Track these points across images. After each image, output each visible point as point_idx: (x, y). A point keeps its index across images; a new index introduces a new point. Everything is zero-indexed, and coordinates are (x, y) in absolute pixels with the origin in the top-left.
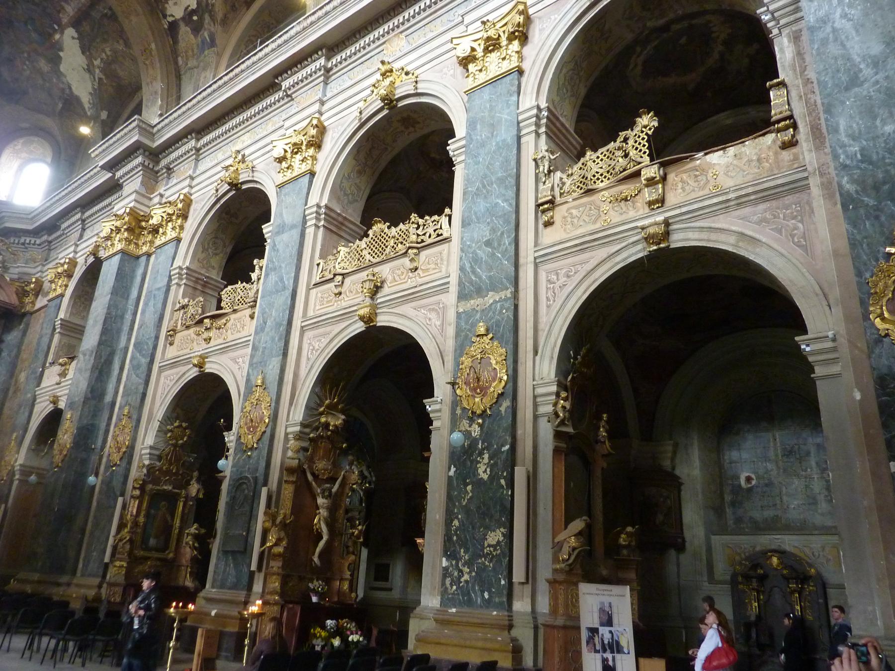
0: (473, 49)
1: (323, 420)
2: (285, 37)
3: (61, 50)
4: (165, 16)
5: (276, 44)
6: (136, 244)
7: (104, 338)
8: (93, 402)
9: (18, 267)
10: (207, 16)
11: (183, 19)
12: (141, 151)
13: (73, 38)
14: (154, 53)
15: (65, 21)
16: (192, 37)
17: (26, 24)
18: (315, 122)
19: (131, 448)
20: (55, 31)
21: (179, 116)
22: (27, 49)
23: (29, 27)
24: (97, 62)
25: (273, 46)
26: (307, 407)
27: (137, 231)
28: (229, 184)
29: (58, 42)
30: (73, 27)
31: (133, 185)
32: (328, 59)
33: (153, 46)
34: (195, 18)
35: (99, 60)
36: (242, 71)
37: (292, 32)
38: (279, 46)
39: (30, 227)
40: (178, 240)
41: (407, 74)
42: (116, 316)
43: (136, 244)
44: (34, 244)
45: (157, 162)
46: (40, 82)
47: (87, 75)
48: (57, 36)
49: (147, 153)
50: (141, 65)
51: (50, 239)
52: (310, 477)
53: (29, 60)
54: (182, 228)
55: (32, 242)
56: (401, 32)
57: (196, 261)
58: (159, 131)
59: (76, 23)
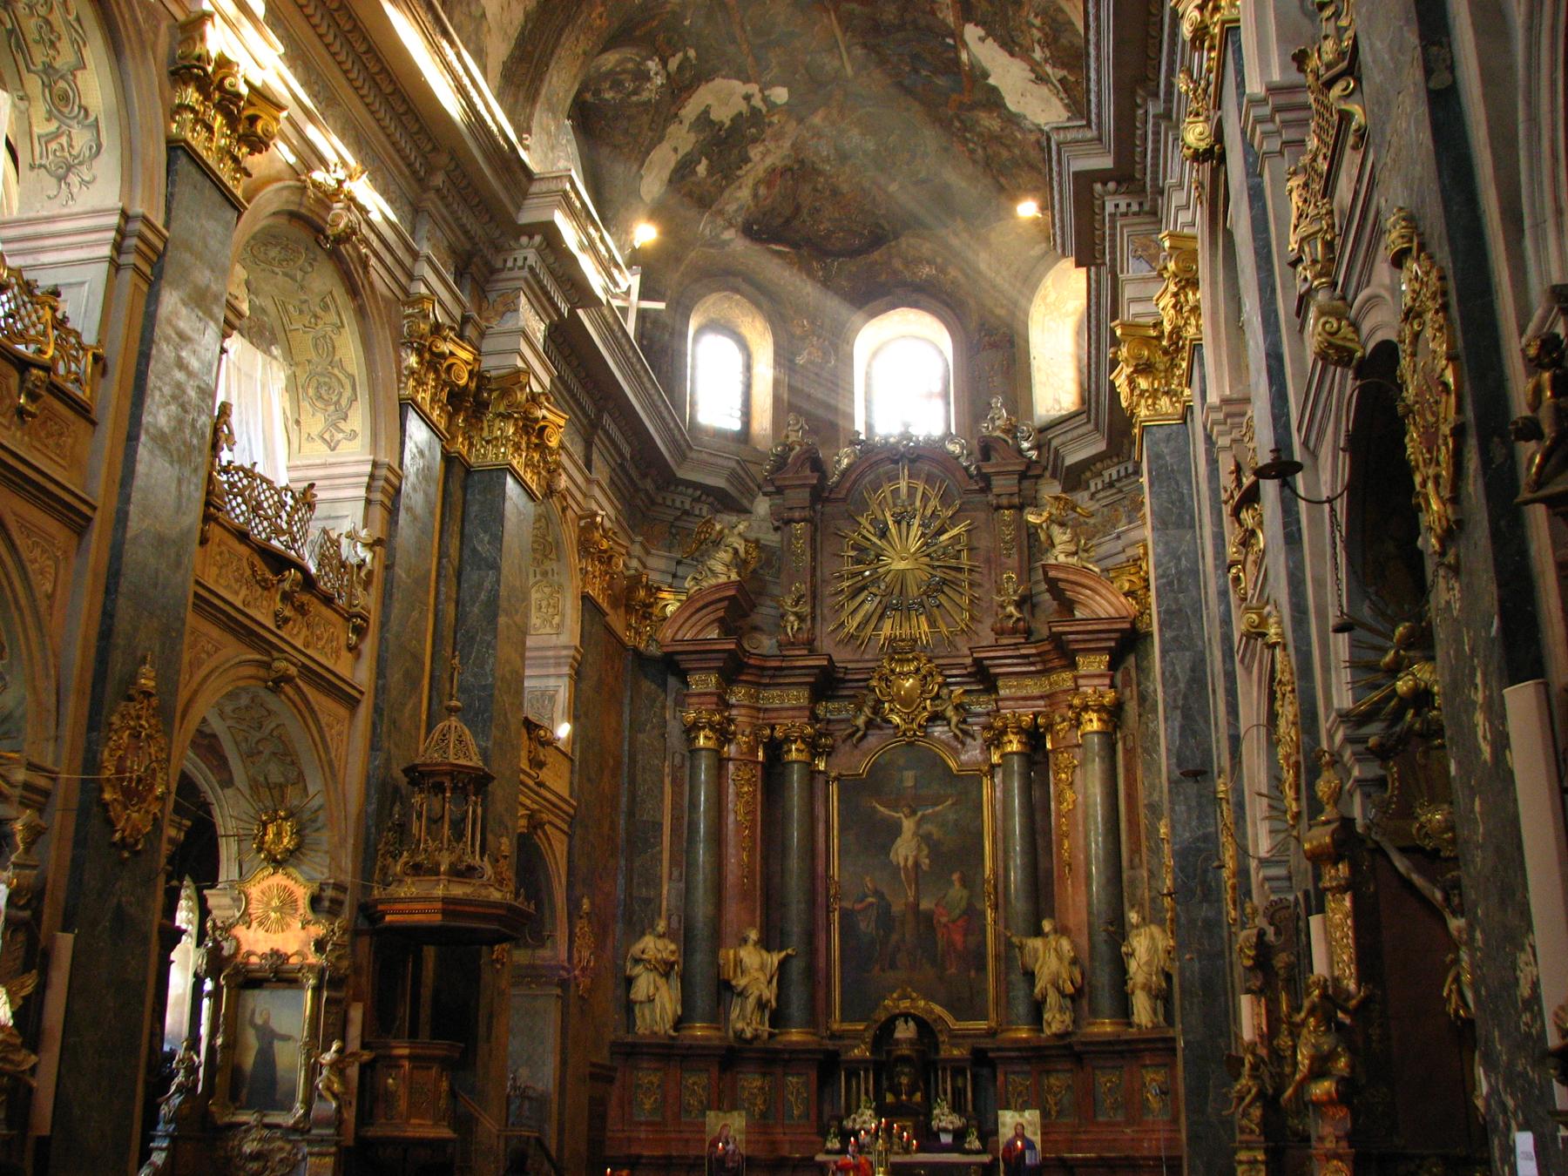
1: (1402, 686)
3: (986, 75)
7: (1168, 635)
8: (1191, 788)
9: (1118, 537)
12: (1098, 187)
13: (982, 40)
15: (951, 20)
17: (917, 72)
19: (1242, 873)
20: (955, 48)
22: (951, 113)
23: (924, 73)
24: (1038, 55)
26: (1354, 664)
27: (1162, 367)
29: (972, 66)
30: (969, 21)
35: (1037, 47)
39: (1101, 446)
40: (1196, 347)
42: (1180, 573)
44: (1127, 476)
45: (1144, 190)
46: (1005, 154)
47: (1044, 90)
48: (964, 56)
49: (1111, 186)
52: (1401, 863)
53: (966, 130)
54: (1195, 309)
55: (1122, 473)
59: (967, 12)
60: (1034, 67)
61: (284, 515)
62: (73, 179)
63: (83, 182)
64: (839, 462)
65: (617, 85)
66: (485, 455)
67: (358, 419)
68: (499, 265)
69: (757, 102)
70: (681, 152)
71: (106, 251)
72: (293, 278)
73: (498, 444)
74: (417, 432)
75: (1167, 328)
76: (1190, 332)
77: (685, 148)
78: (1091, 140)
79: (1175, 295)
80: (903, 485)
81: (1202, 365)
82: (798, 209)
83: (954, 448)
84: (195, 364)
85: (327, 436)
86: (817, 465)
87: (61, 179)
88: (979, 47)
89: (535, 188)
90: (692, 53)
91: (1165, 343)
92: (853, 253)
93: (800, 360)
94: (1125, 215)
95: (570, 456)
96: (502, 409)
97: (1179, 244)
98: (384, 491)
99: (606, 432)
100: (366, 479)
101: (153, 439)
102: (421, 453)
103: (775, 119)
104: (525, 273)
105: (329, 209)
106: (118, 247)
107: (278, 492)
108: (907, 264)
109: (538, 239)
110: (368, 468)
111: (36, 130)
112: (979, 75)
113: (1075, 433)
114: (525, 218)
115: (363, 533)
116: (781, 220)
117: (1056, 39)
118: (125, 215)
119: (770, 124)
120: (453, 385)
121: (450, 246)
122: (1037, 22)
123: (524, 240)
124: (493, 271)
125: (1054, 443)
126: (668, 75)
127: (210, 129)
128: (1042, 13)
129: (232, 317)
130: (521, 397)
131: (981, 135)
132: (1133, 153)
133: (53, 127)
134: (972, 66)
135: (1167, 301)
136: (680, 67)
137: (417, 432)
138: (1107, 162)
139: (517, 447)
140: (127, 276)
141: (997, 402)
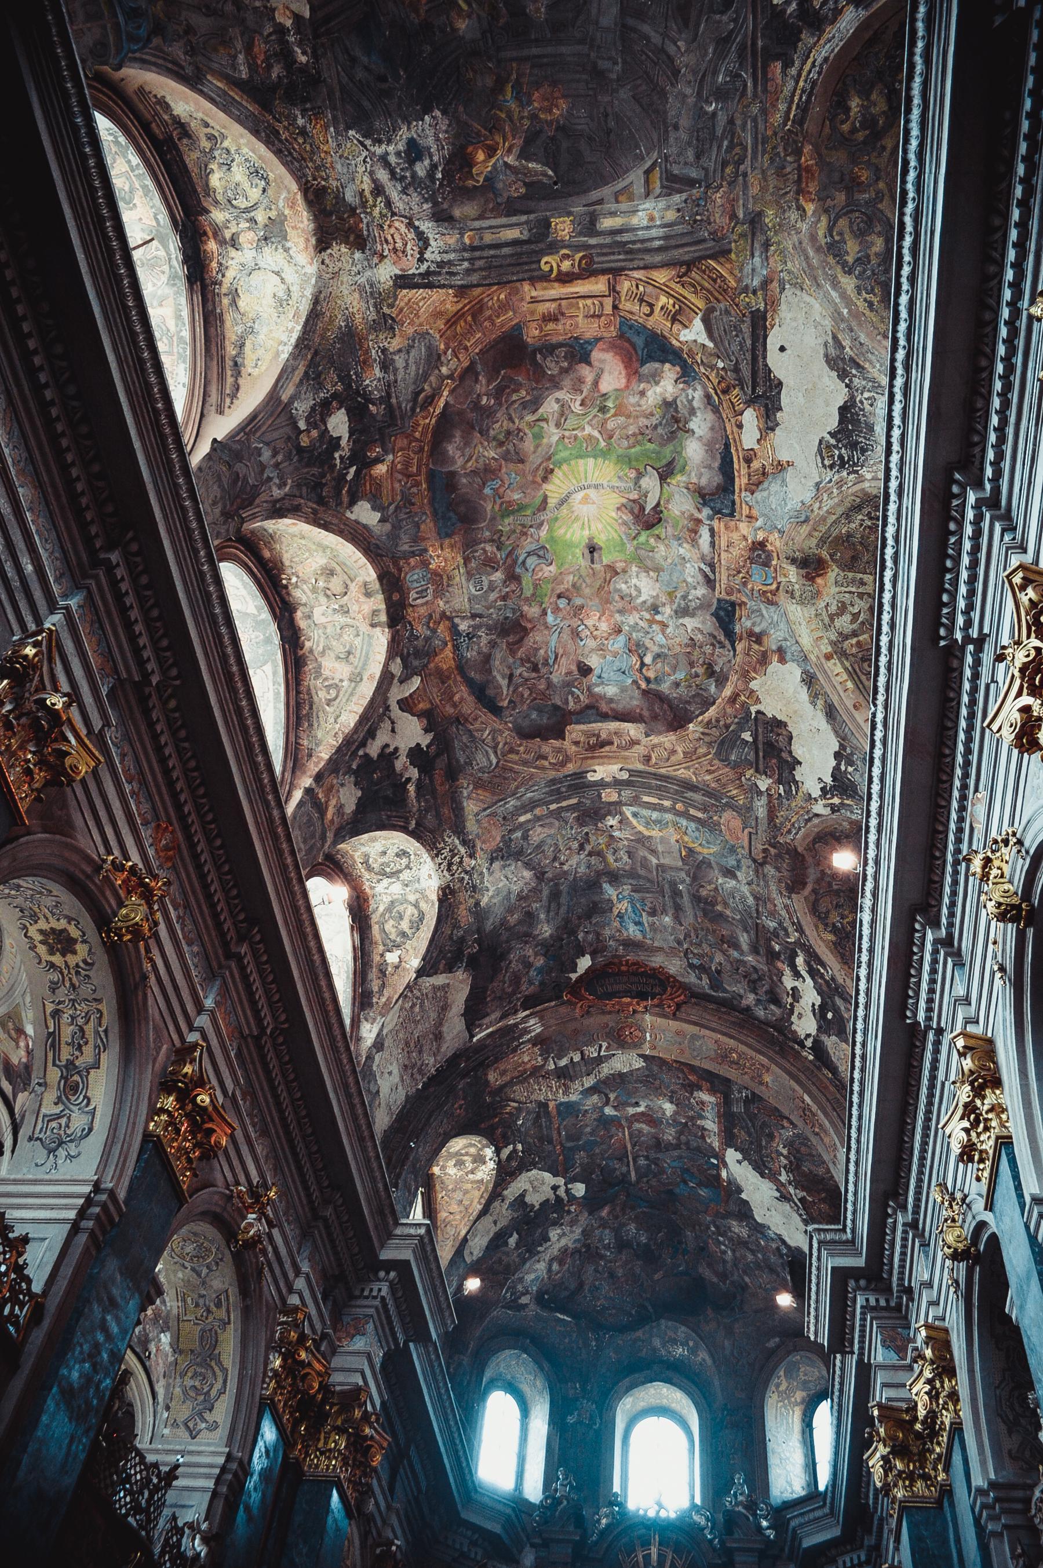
0: (1026, 710)
2: (865, 945)
3: (740, 1190)
4: (803, 1046)
5: (864, 966)
6: (926, 1477)
10: (838, 1001)
11: (820, 1029)
12: (852, 1283)
14: (814, 1108)
15: (716, 1145)
16: (844, 1045)
17: (685, 1182)
18: (960, 1043)
20: (717, 1167)
21: (856, 1185)
24: (783, 1178)
25: (863, 972)
27: (915, 1450)
28: (956, 1256)
29: (729, 1182)
31: (880, 1355)
32: (936, 924)
33: (806, 1098)
34: (830, 1015)
36: (864, 1045)
37: (866, 931)
38: (870, 964)
39: (836, 1532)
40: (957, 1428)
41: (1006, 842)
43: (926, 1477)
45: (889, 1289)
46: (750, 1257)
47: (787, 1207)
48: (724, 1174)
49: (862, 1283)
50: (814, 1140)
51: (873, 1542)
54: (954, 1396)
56: (976, 790)
57: (1007, 1459)
58: (853, 1231)
59: (729, 1140)
60: (780, 1186)
61: (146, 1494)
62: (62, 1153)
63: (70, 1157)
64: (599, 1521)
65: (460, 1164)
66: (317, 1466)
67: (222, 1412)
68: (357, 1293)
69: (561, 1192)
70: (499, 1226)
71: (72, 1214)
72: (199, 1275)
73: (328, 1458)
74: (269, 1433)
75: (921, 1412)
76: (947, 1418)
77: (503, 1223)
78: (847, 1241)
79: (929, 1382)
80: (654, 1557)
81: (963, 1448)
82: (581, 1285)
83: (699, 1519)
84: (115, 1329)
85: (191, 1425)
86: (579, 1521)
87: (51, 1151)
88: (736, 1167)
89: (398, 1231)
90: (520, 1147)
91: (918, 1426)
92: (623, 1329)
93: (571, 1420)
94: (873, 1309)
95: (379, 1480)
96: (339, 1423)
97: (933, 1334)
98: (230, 1486)
99: (411, 1466)
100: (217, 1471)
101: (62, 1392)
102: (267, 1452)
103: (573, 1208)
104: (377, 1302)
105: (245, 1218)
106: (82, 1213)
107: (147, 1468)
108: (664, 1346)
109: (392, 1274)
110: (221, 1460)
111: (43, 1111)
112: (733, 1189)
113: (811, 1516)
114: (385, 1255)
115: (204, 1526)
116: (566, 1293)
117: (798, 1167)
118: (97, 1187)
119: (569, 1212)
120: (305, 1393)
121: (323, 1269)
122: (785, 1152)
123: (382, 1274)
124: (352, 1297)
125: (793, 1524)
126: (499, 1163)
127: (177, 1131)
128: (789, 1144)
129: (152, 1292)
130: (358, 1414)
131: (731, 1239)
132: (882, 1255)
133: (61, 1107)
134: (729, 1182)
135: (920, 1388)
136: (510, 1157)
137: (269, 1433)
138: (860, 1262)
139: (345, 1463)
140: (82, 1238)
141: (739, 1478)
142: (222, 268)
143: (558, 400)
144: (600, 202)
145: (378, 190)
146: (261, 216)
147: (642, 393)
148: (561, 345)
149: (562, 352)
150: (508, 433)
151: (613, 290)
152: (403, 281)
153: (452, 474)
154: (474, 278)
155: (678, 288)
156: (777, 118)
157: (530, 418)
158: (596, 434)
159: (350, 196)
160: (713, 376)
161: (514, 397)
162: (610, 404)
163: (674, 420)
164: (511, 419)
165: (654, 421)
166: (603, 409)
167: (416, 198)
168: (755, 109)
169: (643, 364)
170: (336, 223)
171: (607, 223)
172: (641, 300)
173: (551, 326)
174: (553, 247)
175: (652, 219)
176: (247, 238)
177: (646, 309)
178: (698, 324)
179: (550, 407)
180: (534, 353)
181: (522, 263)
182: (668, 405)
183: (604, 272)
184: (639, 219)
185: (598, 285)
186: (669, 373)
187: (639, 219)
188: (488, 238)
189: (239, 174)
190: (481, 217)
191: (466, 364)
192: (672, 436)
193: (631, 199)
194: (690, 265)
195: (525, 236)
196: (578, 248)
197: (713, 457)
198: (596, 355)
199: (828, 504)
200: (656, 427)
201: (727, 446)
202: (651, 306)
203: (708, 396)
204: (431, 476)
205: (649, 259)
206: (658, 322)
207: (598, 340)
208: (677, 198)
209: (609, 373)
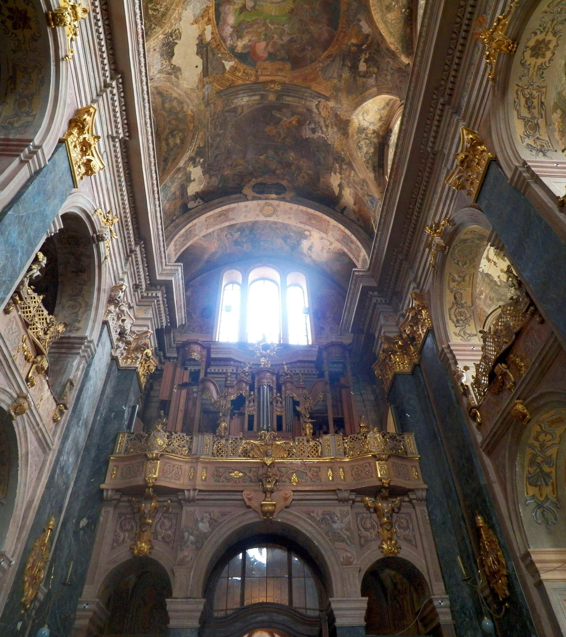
142: (381, 127)
143: (283, 40)
144: (258, 104)
145: (327, 126)
146: (364, 136)
147: (250, 41)
148: (278, 60)
149: (278, 58)
150: (303, 33)
151: (257, 77)
152: (327, 99)
153: (328, 25)
154: (304, 90)
155: (234, 79)
156: (201, 134)
157: (294, 36)
158: (270, 25)
159: (336, 129)
160: (222, 50)
161: (299, 46)
162: (263, 37)
163: (238, 31)
164: (301, 38)
165: (246, 30)
166: (266, 35)
167: (316, 119)
168: (208, 134)
169: (249, 52)
170: (343, 125)
171: (257, 98)
172: (247, 74)
173: (281, 67)
174: (276, 92)
175: (242, 100)
176: (370, 131)
177: (246, 71)
178: (227, 68)
179: (286, 38)
180: (289, 59)
181: (287, 90)
182: (240, 37)
183: (260, 83)
184: (245, 99)
185: (262, 79)
186: (239, 49)
187: (245, 99)
188: (297, 99)
189: (365, 149)
190: (297, 107)
191: (313, 64)
192: (240, 24)
193: (248, 105)
194: (230, 86)
195: (284, 97)
196: (268, 91)
197: (223, 18)
198: (266, 55)
199: (176, 15)
200: (246, 28)
201: (218, 24)
202: (244, 72)
203: (225, 42)
204: (336, 28)
205: (244, 87)
206: (242, 67)
207: (265, 60)
208: (233, 106)
209: (261, 48)
